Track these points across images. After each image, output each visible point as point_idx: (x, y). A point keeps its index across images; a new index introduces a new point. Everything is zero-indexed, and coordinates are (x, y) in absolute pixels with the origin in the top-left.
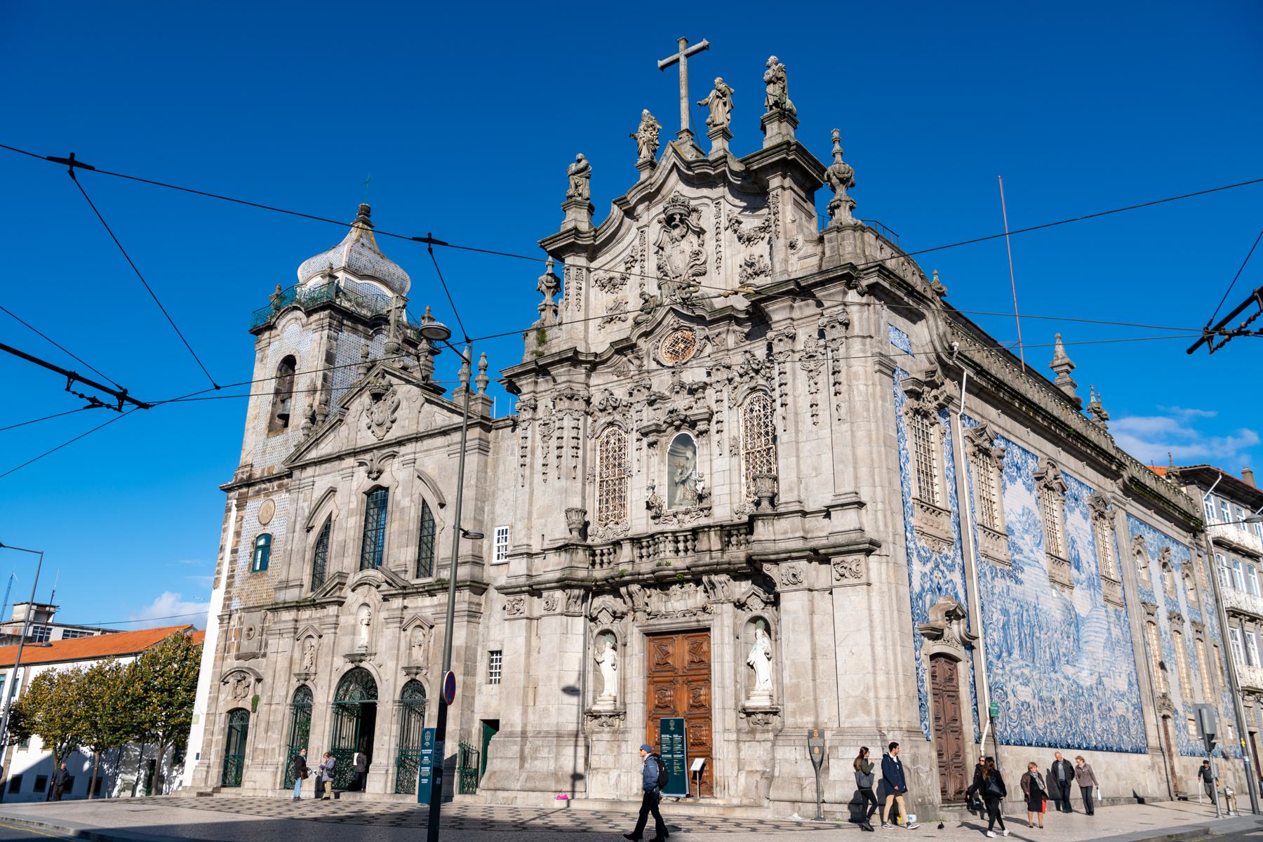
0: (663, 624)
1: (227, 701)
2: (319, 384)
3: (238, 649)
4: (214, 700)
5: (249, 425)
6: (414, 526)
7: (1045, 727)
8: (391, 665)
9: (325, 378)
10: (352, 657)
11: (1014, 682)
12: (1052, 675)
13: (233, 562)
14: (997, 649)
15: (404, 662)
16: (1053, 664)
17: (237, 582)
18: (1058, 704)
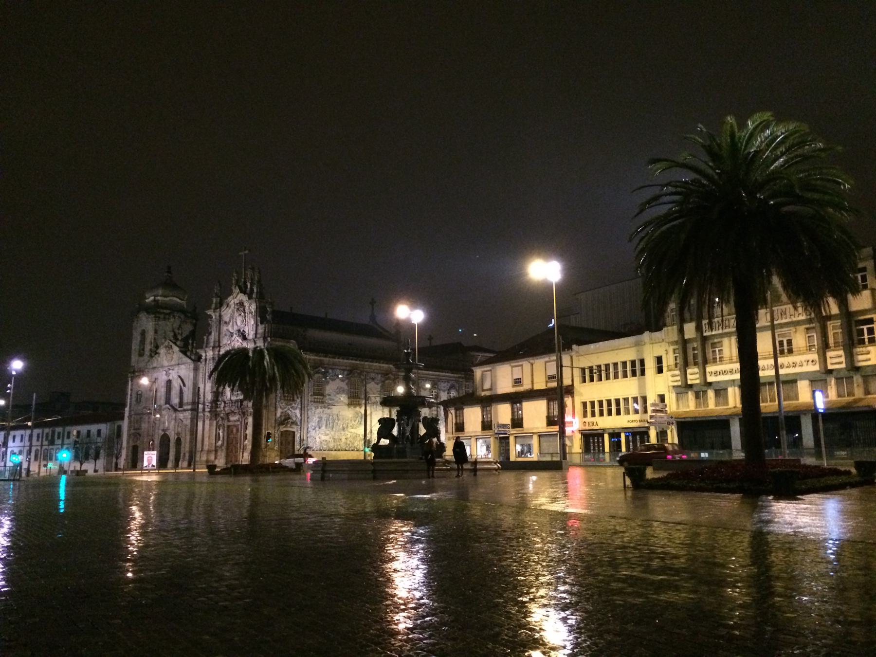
0: (230, 424)
1: (132, 444)
2: (153, 341)
3: (134, 427)
4: (128, 442)
5: (133, 352)
6: (178, 392)
7: (334, 446)
8: (173, 432)
9: (155, 339)
10: (163, 430)
11: (320, 435)
12: (343, 432)
13: (131, 399)
14: (313, 428)
15: (176, 432)
16: (344, 429)
17: (133, 404)
18: (343, 440)
